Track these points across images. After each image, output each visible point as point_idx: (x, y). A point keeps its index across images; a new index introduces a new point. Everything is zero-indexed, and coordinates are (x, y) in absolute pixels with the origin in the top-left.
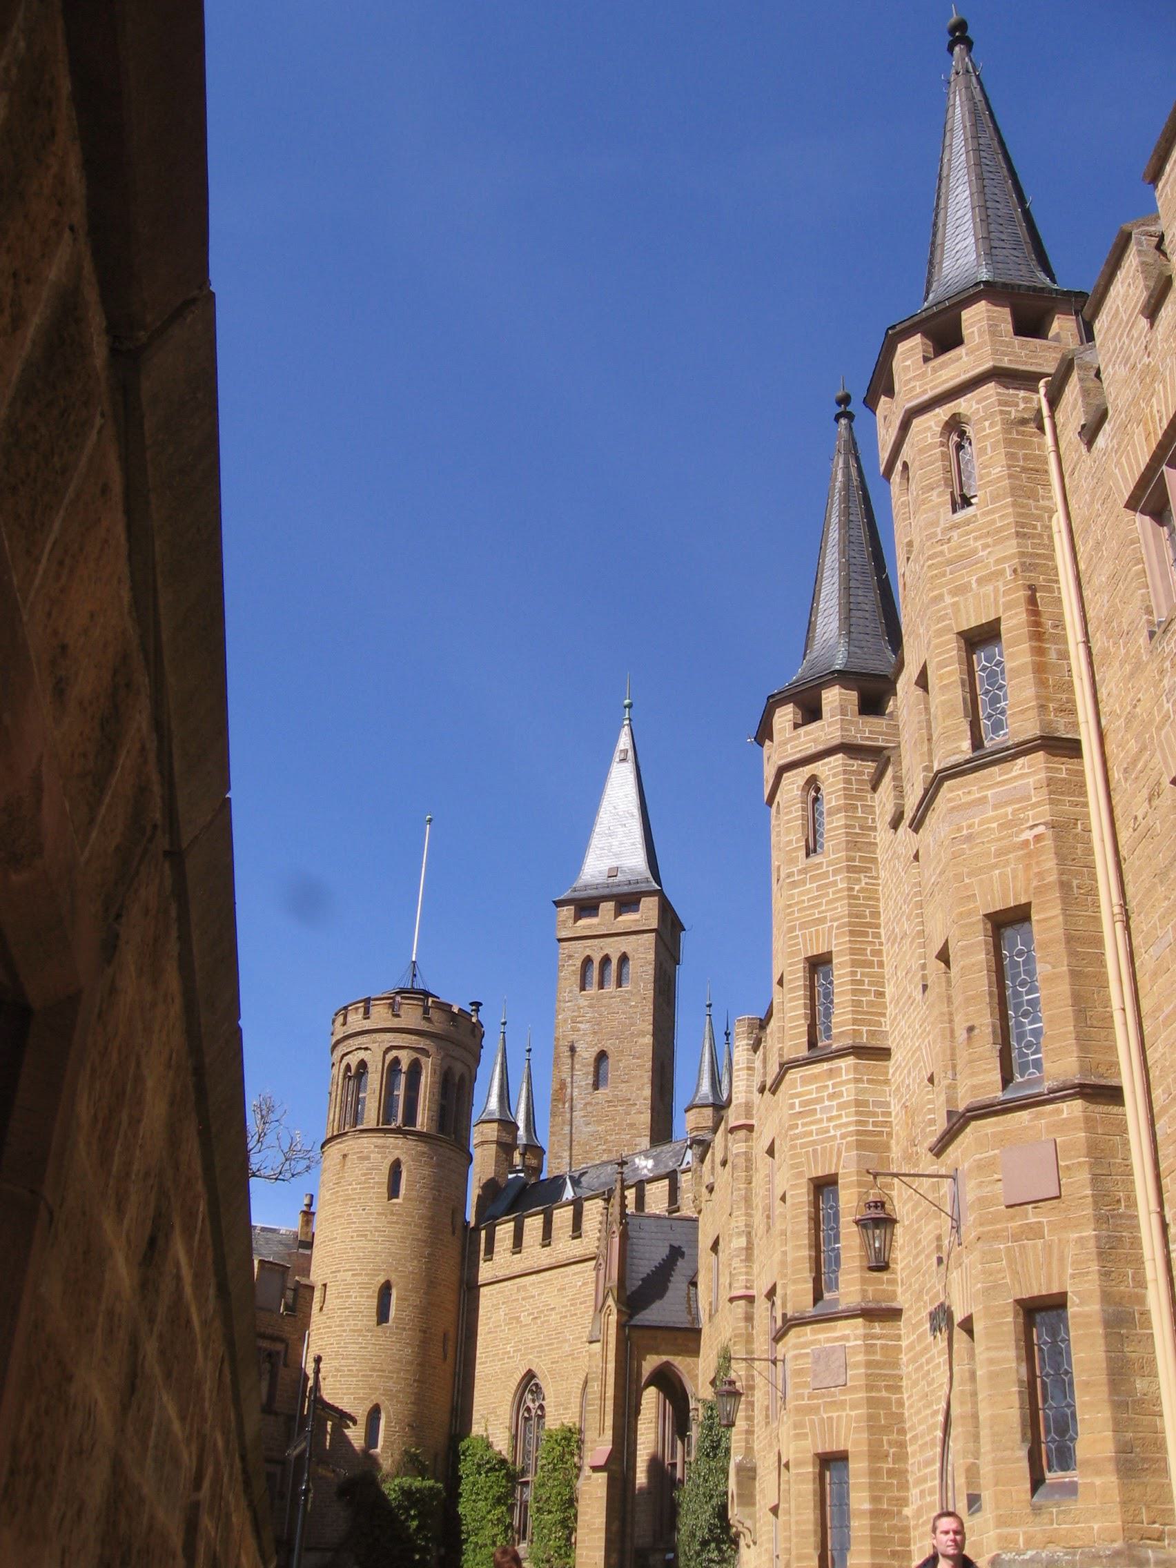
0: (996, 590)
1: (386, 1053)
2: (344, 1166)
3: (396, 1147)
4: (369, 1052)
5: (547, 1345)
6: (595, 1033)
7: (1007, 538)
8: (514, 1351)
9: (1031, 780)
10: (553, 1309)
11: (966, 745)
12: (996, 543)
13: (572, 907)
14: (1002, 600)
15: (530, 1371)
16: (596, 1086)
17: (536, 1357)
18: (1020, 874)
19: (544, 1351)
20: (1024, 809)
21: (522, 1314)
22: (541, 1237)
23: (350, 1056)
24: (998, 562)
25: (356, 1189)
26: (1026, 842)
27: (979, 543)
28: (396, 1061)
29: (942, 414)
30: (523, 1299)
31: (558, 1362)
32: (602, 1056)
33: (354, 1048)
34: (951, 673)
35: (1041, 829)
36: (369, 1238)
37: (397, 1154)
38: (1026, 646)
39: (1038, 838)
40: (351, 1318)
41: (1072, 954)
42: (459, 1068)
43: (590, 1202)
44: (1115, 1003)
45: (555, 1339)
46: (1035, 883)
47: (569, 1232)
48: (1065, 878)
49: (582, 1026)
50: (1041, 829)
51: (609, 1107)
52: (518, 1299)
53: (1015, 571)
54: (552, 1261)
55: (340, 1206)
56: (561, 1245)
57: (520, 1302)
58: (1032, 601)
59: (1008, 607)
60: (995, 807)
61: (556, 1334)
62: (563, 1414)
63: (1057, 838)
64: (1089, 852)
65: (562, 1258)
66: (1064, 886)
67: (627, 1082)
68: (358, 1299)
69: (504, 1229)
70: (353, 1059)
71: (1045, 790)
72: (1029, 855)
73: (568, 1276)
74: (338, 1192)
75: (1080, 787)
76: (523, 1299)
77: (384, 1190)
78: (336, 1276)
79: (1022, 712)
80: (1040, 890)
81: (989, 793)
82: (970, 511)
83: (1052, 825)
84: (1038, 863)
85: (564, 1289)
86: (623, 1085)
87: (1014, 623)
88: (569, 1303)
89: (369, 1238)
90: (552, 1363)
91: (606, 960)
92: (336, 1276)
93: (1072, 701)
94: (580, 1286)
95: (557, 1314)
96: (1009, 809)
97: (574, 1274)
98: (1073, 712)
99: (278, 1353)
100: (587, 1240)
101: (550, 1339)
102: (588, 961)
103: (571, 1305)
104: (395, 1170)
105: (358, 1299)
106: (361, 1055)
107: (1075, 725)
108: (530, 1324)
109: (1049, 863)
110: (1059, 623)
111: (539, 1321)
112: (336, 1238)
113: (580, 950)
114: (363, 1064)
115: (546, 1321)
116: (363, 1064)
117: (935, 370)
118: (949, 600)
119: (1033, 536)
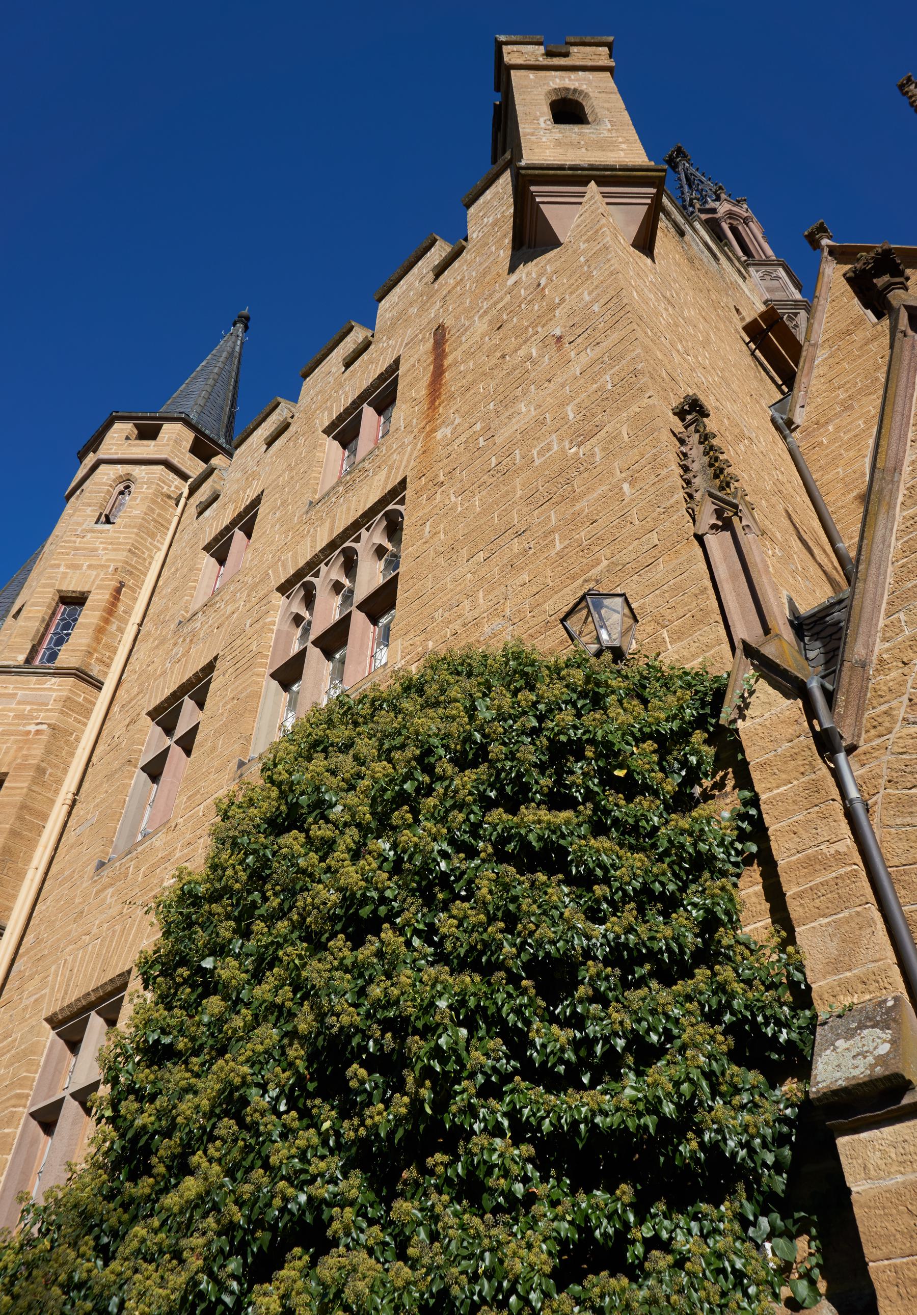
0: (97, 576)
7: (122, 550)
9: (55, 694)
11: (21, 658)
12: (113, 550)
14: (98, 582)
18: (12, 752)
20: (40, 711)
24: (108, 560)
26: (30, 732)
27: (102, 546)
29: (121, 469)
34: (39, 611)
35: (44, 727)
38: (98, 613)
39: (38, 732)
41: (20, 818)
44: (34, 863)
46: (19, 761)
48: (43, 765)
50: (44, 727)
53: (116, 569)
58: (118, 591)
59: (99, 587)
60: (19, 703)
63: (53, 736)
64: (72, 754)
66: (40, 770)
71: (61, 703)
72: (25, 742)
75: (88, 713)
79: (73, 651)
80: (19, 767)
81: (20, 692)
82: (108, 526)
83: (53, 727)
84: (29, 749)
87: (98, 599)
93: (111, 659)
96: (28, 708)
98: (108, 666)
107: (106, 674)
109: (38, 751)
110: (128, 612)
117: (129, 446)
118: (62, 569)
119: (139, 557)
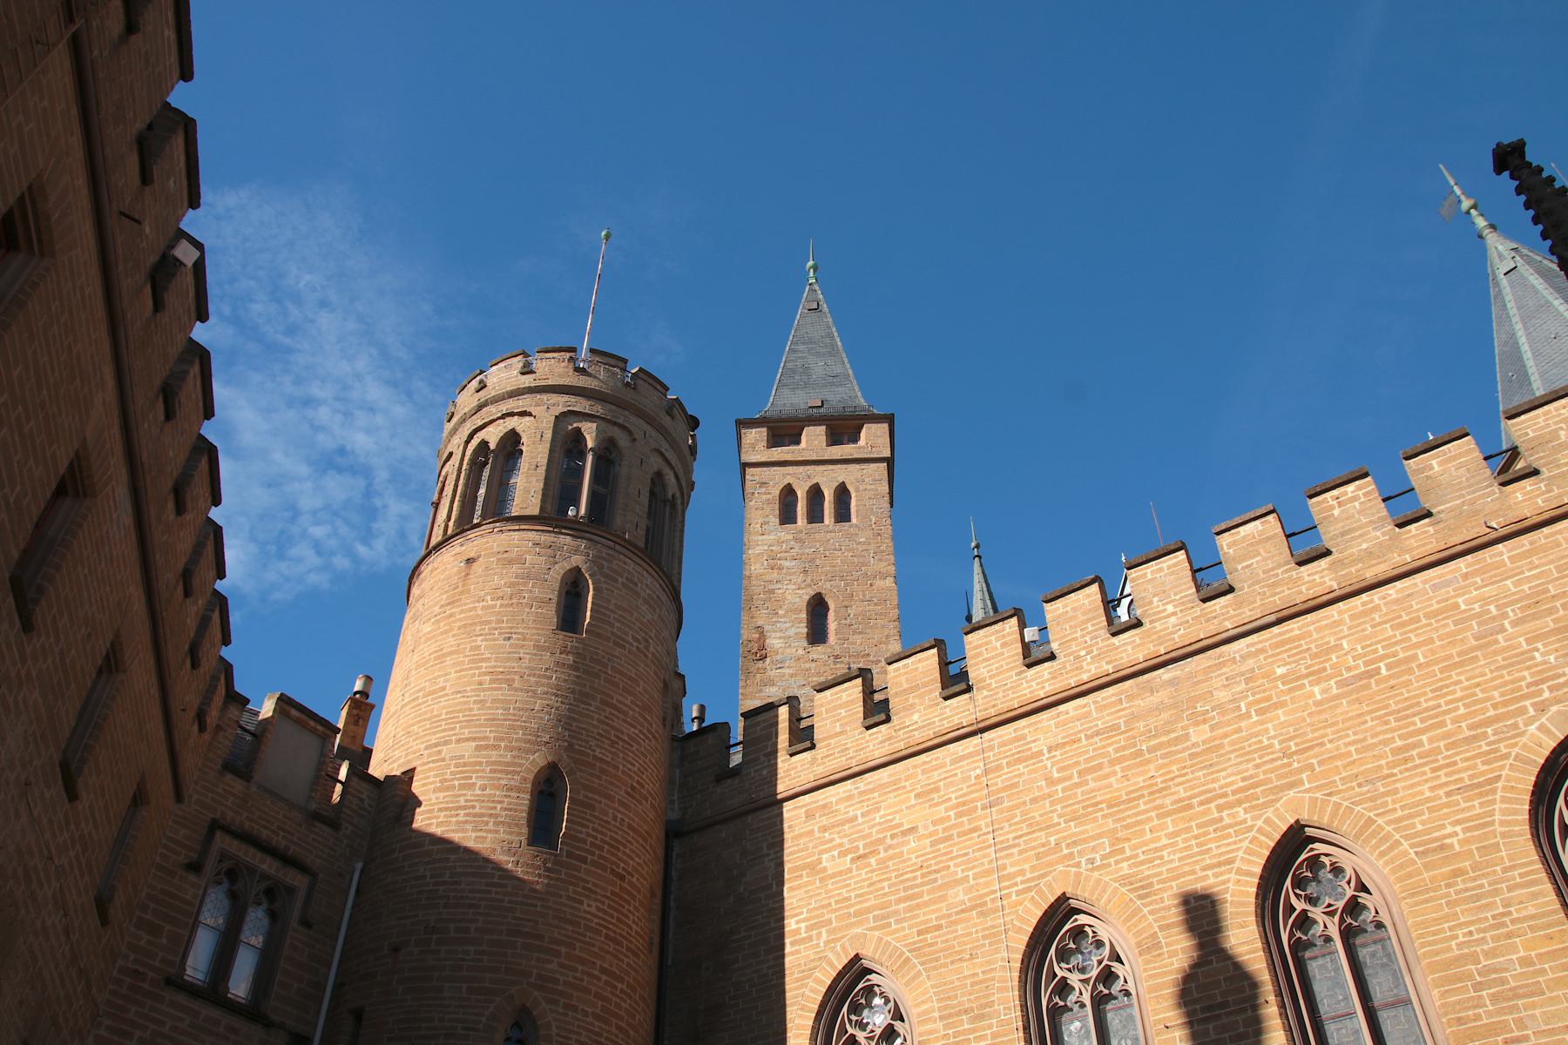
1: (560, 419)
2: (468, 574)
3: (576, 551)
4: (527, 418)
5: (899, 901)
6: (805, 572)
8: (809, 928)
10: (913, 830)
13: (765, 429)
15: (857, 958)
16: (817, 634)
17: (870, 929)
19: (896, 912)
21: (825, 856)
22: (861, 715)
23: (490, 429)
25: (494, 606)
28: (578, 436)
30: (824, 829)
31: (939, 927)
32: (818, 608)
33: (500, 415)
36: (516, 685)
37: (577, 560)
40: (469, 827)
42: (670, 478)
43: (982, 632)
45: (922, 885)
47: (931, 691)
49: (786, 564)
51: (835, 663)
52: (812, 831)
54: (900, 746)
55: (454, 636)
56: (916, 717)
57: (817, 835)
61: (923, 876)
62: (974, 1031)
65: (920, 737)
67: (861, 633)
68: (488, 792)
69: (764, 721)
70: (493, 435)
73: (943, 766)
74: (451, 615)
76: (824, 829)
77: (550, 613)
78: (440, 752)
85: (937, 790)
86: (857, 636)
88: (951, 813)
89: (516, 685)
90: (920, 933)
91: (816, 494)
92: (440, 752)
94: (977, 777)
95: (920, 838)
97: (954, 762)
99: (291, 891)
100: (985, 693)
101: (905, 889)
102: (788, 493)
103: (959, 815)
104: (572, 590)
105: (488, 792)
106: (512, 423)
108: (850, 870)
111: (873, 861)
112: (443, 688)
113: (779, 478)
114: (512, 439)
115: (891, 858)
116: (512, 439)
